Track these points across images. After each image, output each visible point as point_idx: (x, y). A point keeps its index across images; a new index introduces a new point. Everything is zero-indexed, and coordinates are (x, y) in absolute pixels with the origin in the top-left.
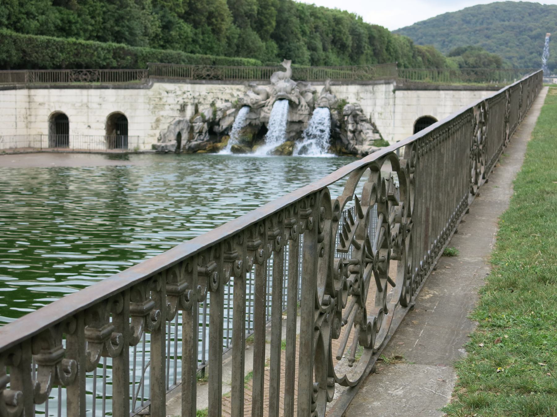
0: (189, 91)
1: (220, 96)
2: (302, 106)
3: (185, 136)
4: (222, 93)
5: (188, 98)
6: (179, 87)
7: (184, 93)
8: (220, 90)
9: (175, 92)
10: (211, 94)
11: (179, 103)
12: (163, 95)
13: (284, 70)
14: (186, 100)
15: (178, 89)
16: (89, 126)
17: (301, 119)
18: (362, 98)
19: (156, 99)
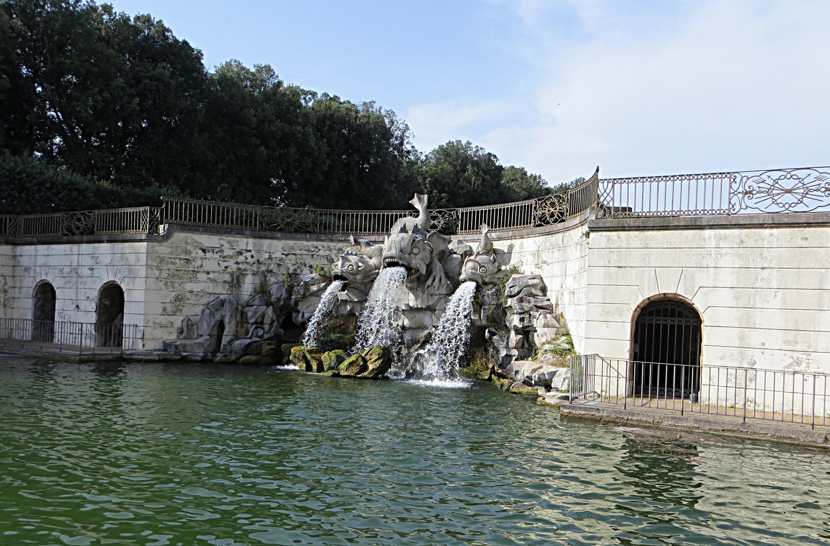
0: (250, 251)
1: (309, 261)
3: (229, 329)
5: (248, 263)
6: (229, 242)
7: (240, 253)
8: (309, 250)
9: (222, 251)
11: (229, 270)
12: (193, 255)
13: (416, 213)
14: (241, 266)
15: (226, 245)
16: (77, 306)
17: (431, 303)
18: (545, 262)
19: (177, 261)
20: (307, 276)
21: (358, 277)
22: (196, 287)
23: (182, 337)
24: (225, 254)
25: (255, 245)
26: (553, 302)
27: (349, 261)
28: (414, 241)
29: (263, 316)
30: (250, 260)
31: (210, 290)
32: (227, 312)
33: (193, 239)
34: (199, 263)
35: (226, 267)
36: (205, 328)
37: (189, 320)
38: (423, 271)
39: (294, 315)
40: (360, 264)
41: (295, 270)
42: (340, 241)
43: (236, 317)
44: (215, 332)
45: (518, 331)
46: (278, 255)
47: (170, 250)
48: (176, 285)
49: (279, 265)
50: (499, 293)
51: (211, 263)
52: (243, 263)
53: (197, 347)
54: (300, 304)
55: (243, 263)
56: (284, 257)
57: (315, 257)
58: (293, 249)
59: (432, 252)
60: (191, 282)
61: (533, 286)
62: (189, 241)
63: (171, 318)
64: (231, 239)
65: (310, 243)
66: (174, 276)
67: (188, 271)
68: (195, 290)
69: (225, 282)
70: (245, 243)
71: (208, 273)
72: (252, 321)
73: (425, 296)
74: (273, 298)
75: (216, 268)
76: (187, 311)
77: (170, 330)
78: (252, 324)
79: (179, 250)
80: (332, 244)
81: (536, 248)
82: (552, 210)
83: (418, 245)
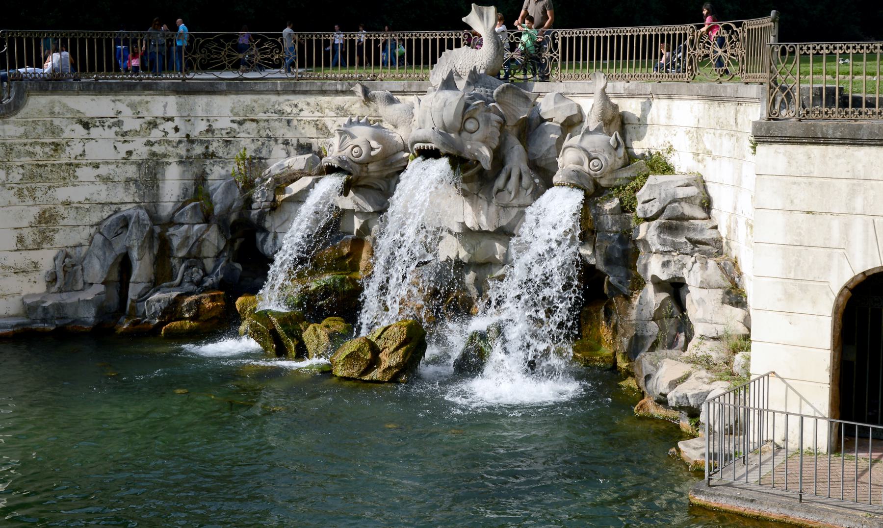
0: (171, 119)
2: (509, 178)
3: (141, 269)
4: (289, 122)
5: (169, 142)
6: (132, 106)
7: (153, 124)
8: (281, 112)
9: (119, 124)
10: (249, 125)
11: (134, 157)
12: (67, 134)
13: (474, 40)
14: (156, 149)
15: (127, 112)
17: (504, 222)
18: (709, 153)
19: (38, 149)
20: (281, 161)
21: (372, 167)
22: (76, 194)
23: (54, 289)
24: (126, 128)
25: (180, 107)
26: (723, 232)
27: (353, 137)
28: (467, 106)
29: (200, 242)
30: (173, 136)
31: (103, 198)
32: (133, 240)
33: (64, 106)
34: (77, 149)
35: (129, 153)
36: (96, 269)
37: (67, 256)
38: (487, 165)
39: (260, 237)
40: (374, 144)
41: (258, 150)
42: (337, 93)
43: (151, 247)
44: (115, 276)
45: (659, 285)
46: (224, 123)
47: (22, 130)
48: (38, 194)
49: (227, 142)
50: (625, 208)
51: (102, 147)
52: (159, 143)
53: (85, 301)
54: (268, 218)
55: (159, 143)
56: (235, 126)
57: (295, 122)
58: (253, 110)
59: (503, 124)
60: (66, 185)
61: (688, 200)
62: (56, 109)
63: (35, 256)
64: (136, 98)
65: (282, 98)
66: (32, 177)
67: (61, 165)
68: (75, 199)
69: (128, 181)
70: (162, 105)
71: (97, 166)
72: (181, 254)
73: (493, 209)
74: (217, 209)
75: (111, 155)
76: (63, 239)
77: (32, 276)
78: (183, 259)
79: (40, 129)
80: (323, 100)
81: (693, 123)
82: (720, 52)
83: (476, 115)
